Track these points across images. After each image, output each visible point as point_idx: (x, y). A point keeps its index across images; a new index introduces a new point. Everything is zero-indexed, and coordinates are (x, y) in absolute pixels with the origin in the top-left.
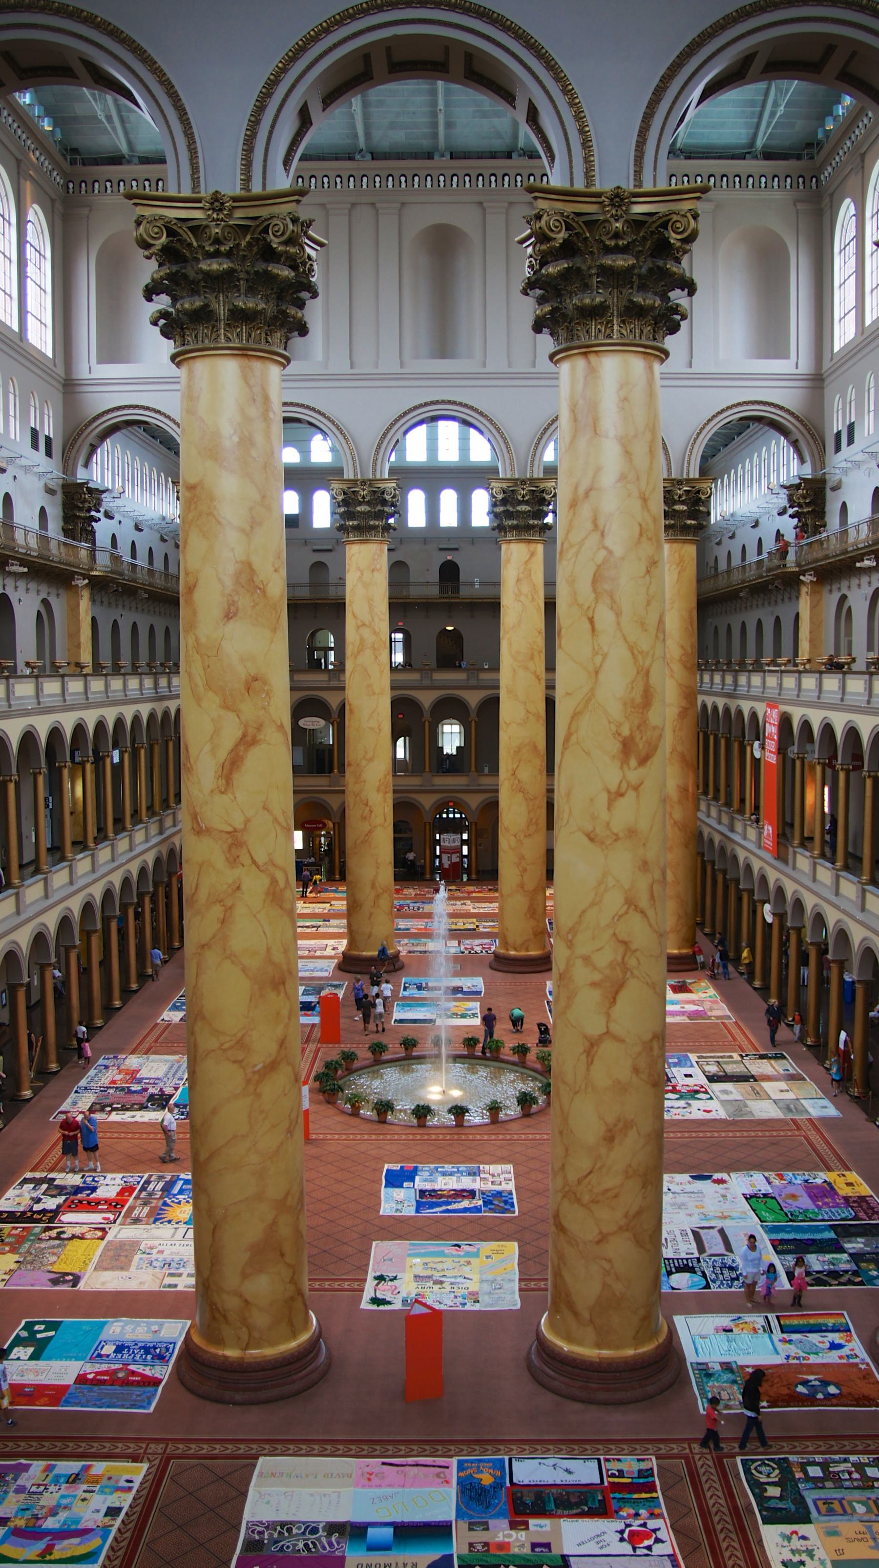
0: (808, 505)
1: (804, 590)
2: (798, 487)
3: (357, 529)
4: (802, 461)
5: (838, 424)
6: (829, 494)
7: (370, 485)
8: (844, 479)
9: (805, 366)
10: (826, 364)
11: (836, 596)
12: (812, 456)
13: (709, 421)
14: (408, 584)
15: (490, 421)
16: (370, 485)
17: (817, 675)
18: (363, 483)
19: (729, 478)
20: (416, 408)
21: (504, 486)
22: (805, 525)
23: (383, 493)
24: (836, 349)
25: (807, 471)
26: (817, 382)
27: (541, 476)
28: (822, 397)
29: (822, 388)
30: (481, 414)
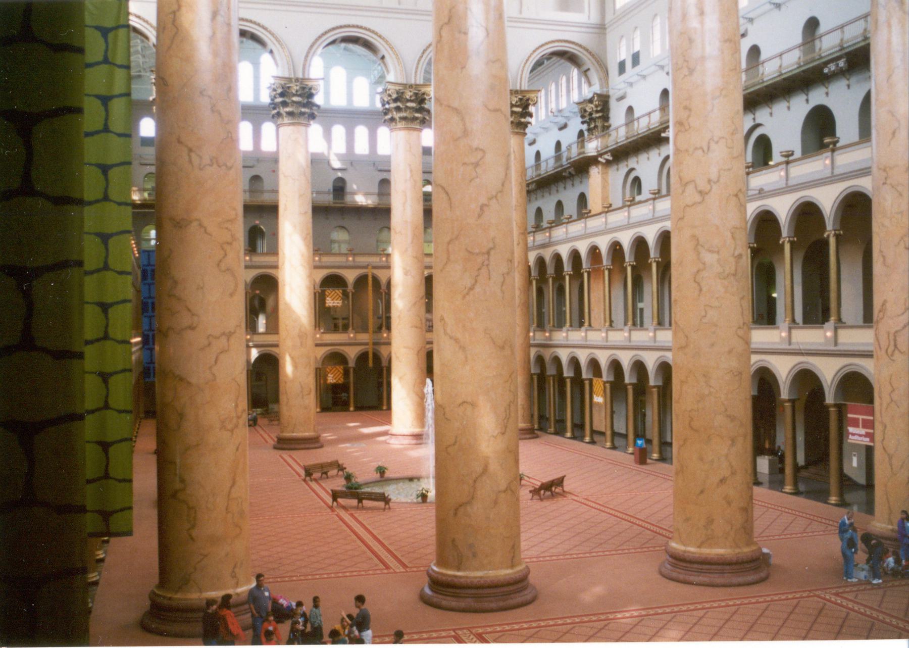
0: (597, 112)
1: (595, 172)
2: (591, 101)
3: (290, 114)
4: (590, 84)
5: (624, 54)
6: (613, 103)
7: (301, 83)
8: (629, 90)
9: (594, 18)
10: (609, 17)
11: (625, 170)
12: (600, 79)
13: (534, 51)
14: (262, 192)
15: (387, 42)
16: (301, 83)
17: (651, 202)
18: (297, 80)
19: (568, 81)
20: (334, 29)
21: (397, 88)
22: (596, 127)
23: (310, 89)
24: (618, 6)
25: (597, 88)
26: (601, 28)
27: (422, 83)
28: (605, 40)
29: (605, 34)
30: (380, 37)
